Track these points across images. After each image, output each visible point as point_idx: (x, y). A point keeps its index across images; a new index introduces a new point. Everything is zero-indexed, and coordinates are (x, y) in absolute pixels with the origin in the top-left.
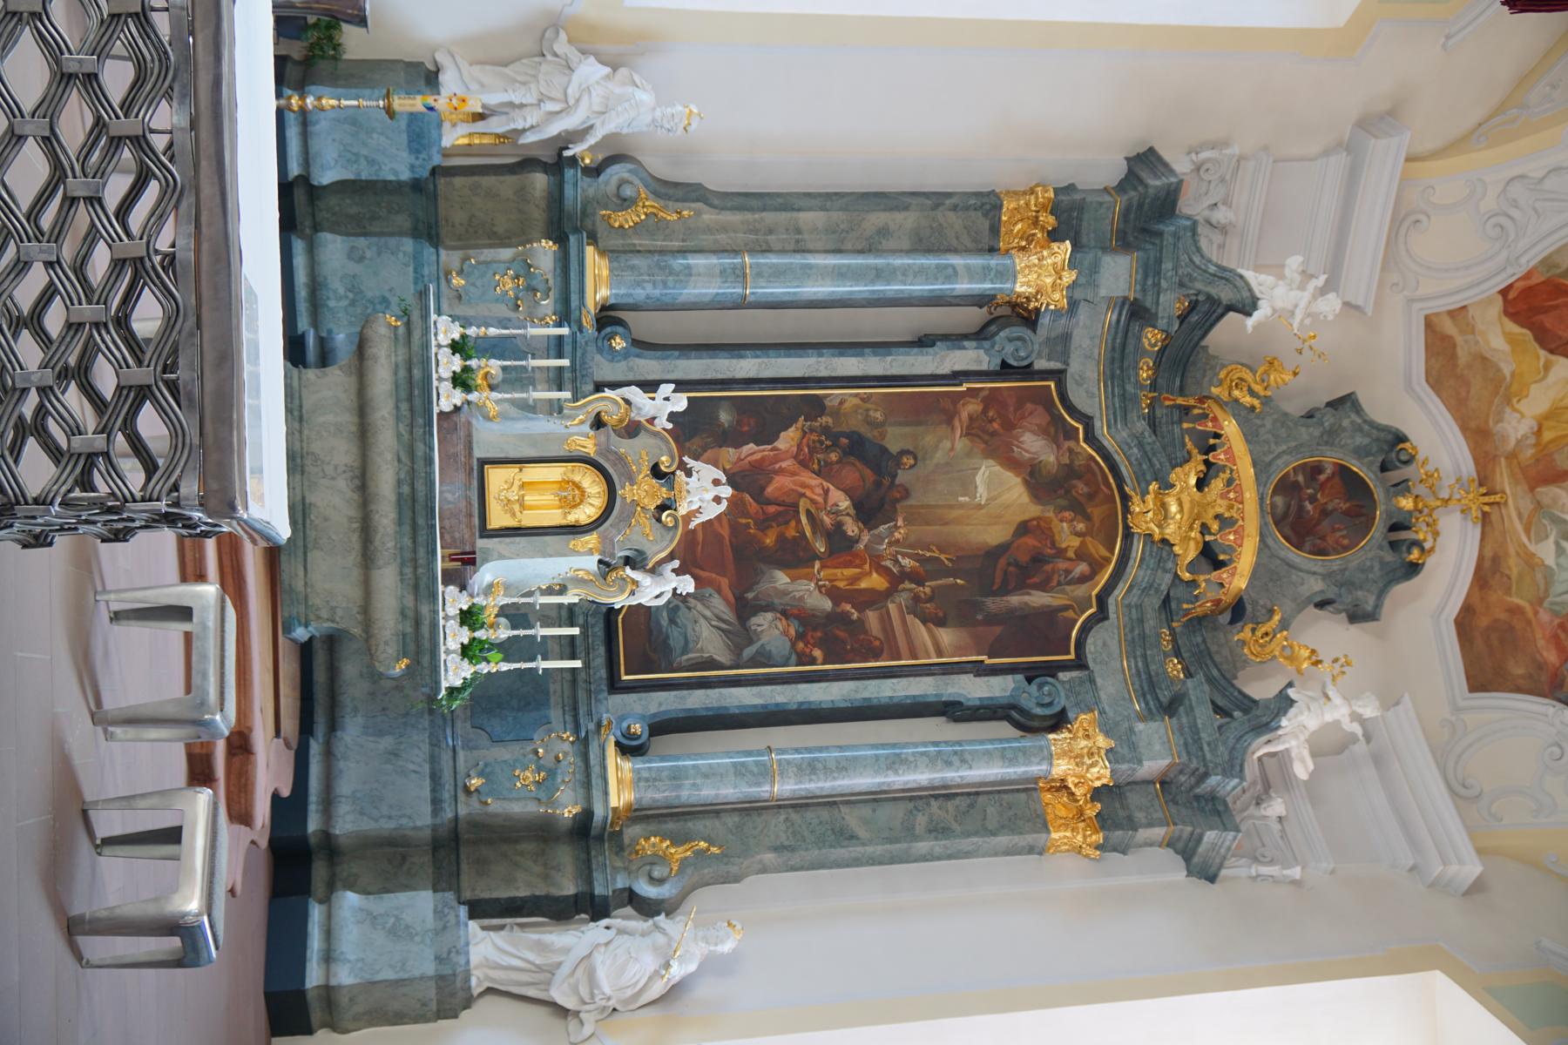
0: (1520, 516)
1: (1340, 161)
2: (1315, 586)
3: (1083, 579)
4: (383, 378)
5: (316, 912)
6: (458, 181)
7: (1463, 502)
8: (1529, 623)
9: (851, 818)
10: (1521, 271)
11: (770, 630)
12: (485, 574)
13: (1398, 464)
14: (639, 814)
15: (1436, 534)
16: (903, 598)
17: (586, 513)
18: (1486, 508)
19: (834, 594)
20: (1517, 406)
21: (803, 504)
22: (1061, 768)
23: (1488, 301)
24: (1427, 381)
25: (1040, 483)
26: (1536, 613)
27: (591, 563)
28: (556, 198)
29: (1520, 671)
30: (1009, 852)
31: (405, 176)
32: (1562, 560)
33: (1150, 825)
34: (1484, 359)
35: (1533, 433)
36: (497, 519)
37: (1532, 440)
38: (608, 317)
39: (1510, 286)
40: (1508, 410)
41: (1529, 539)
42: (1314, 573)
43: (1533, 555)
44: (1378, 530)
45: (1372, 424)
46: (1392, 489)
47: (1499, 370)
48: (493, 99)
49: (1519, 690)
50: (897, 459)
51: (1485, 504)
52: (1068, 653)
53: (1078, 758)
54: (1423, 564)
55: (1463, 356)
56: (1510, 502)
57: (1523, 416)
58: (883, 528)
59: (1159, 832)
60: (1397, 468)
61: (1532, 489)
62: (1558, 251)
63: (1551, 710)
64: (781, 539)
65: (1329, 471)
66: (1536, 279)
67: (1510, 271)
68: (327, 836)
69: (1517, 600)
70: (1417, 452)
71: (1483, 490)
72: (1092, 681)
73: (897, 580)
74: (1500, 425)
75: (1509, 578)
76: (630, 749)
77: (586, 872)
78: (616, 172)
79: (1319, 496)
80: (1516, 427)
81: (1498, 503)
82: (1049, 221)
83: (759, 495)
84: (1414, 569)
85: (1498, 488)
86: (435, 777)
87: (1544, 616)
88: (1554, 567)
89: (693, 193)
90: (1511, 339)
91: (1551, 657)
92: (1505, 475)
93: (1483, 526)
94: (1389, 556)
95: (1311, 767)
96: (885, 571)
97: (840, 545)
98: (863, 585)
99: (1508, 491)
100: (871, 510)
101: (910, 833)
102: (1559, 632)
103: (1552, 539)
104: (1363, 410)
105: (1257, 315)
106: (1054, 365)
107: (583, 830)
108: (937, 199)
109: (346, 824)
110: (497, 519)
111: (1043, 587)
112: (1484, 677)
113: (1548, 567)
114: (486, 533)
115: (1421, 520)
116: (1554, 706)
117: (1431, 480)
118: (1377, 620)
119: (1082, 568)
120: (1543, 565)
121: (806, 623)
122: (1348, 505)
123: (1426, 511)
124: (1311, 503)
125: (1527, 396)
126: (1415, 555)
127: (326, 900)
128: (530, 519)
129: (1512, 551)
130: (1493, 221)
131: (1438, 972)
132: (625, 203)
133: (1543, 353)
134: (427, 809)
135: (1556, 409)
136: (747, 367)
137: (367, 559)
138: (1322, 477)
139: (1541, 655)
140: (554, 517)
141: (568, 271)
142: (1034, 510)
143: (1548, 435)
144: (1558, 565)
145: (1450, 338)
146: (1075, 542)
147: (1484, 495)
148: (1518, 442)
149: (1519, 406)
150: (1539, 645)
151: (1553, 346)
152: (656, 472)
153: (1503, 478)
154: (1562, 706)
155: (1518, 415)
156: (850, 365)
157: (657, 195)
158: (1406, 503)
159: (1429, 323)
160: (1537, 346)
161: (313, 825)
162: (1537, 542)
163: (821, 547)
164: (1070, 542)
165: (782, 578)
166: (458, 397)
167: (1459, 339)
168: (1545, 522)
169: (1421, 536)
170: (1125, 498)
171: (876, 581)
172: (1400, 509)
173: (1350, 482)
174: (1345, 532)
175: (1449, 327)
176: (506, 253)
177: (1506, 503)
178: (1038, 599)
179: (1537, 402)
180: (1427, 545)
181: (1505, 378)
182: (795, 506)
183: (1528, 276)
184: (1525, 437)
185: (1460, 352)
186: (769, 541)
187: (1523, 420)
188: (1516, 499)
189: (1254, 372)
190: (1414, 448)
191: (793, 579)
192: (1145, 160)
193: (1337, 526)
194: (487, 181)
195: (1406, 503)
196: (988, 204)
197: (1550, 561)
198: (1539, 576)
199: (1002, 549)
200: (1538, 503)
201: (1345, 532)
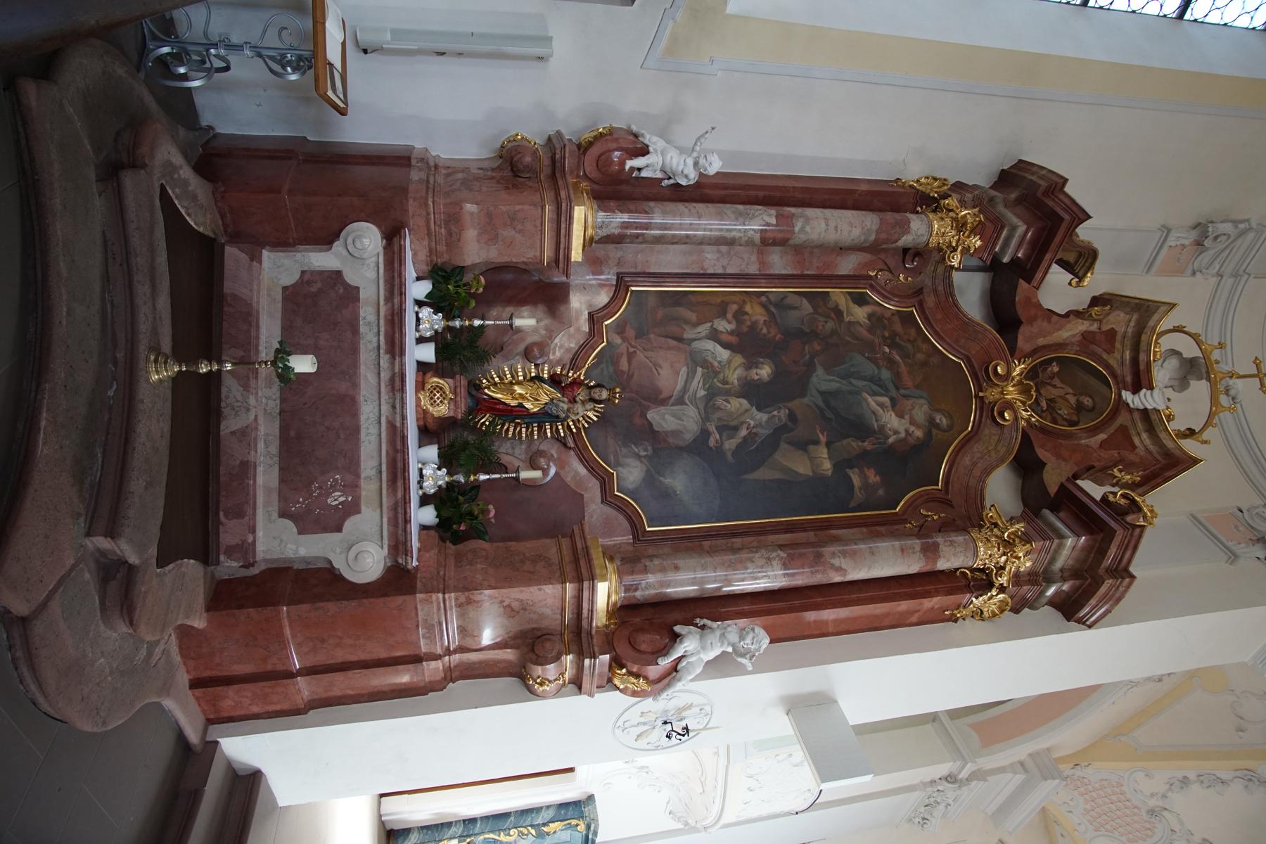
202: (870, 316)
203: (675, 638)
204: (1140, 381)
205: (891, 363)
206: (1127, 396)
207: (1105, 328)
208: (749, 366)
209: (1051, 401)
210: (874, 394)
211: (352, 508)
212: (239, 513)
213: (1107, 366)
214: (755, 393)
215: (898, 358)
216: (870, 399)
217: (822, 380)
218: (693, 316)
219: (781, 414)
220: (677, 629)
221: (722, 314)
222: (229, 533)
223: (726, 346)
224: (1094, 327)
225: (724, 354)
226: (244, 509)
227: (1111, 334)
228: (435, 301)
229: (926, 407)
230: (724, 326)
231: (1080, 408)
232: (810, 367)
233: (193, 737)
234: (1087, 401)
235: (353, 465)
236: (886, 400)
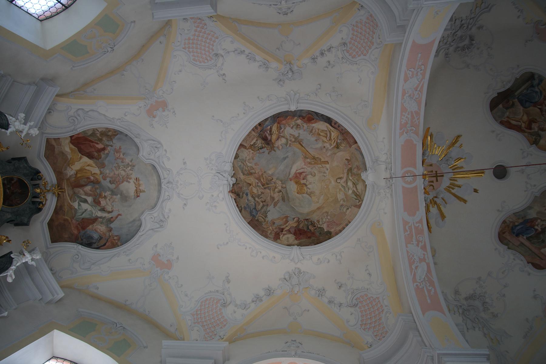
0: (69, 195)
1: (33, 88)
2: (9, 216)
7: (54, 191)
8: (70, 223)
10: (77, 133)
13: (37, 179)
15: (46, 200)
18: (60, 193)
20: (71, 167)
23: (66, 138)
24: (45, 156)
26: (72, 221)
29: (66, 236)
32: (80, 207)
34: (63, 153)
35: (75, 174)
37: (74, 176)
39: (73, 136)
40: (68, 168)
41: (71, 201)
42: (8, 212)
43: (72, 206)
44: (29, 199)
45: (30, 167)
46: (34, 186)
47: (67, 157)
49: (66, 241)
51: (59, 192)
54: (42, 209)
56: (66, 192)
57: (72, 169)
60: (37, 180)
61: (73, 189)
62: (88, 130)
63: (75, 246)
65: (15, 180)
66: (80, 136)
67: (74, 132)
69: (66, 217)
70: (43, 177)
71: (59, 188)
74: (65, 171)
75: (64, 211)
79: (11, 188)
80: (70, 172)
81: (63, 192)
84: (40, 210)
85: (63, 187)
87: (74, 221)
88: (77, 209)
90: (71, 149)
91: (76, 232)
92: (66, 184)
93: (58, 197)
95: (14, 277)
99: (66, 188)
102: (78, 226)
103: (77, 201)
104: (28, 163)
105: (10, 130)
112: (55, 239)
113: (76, 209)
115: (42, 195)
116: (76, 245)
117: (45, 184)
118: (29, 225)
120: (75, 208)
122: (20, 191)
123: (43, 193)
124: (8, 190)
125: (74, 164)
129: (66, 204)
130: (72, 118)
131: (55, 330)
133: (80, 155)
135: (82, 169)
138: (13, 182)
139: (73, 231)
143: (79, 175)
144: (78, 208)
145: (54, 146)
147: (59, 189)
148: (70, 176)
149: (72, 167)
150: (72, 229)
151: (83, 153)
153: (65, 185)
154: (78, 245)
155: (71, 169)
158: (38, 191)
159: (48, 140)
160: (78, 152)
162: (73, 203)
167: (56, 146)
168: (76, 197)
169: (42, 201)
172: (36, 192)
173: (21, 183)
174: (19, 199)
175: (53, 143)
177: (65, 192)
179: (77, 166)
180: (44, 203)
181: (68, 159)
183: (78, 134)
184: (72, 175)
185: (56, 150)
187: (72, 171)
188: (68, 191)
190: (42, 175)
193: (17, 197)
195: (38, 191)
197: (76, 207)
198: (73, 211)
200: (74, 192)
201: (19, 199)
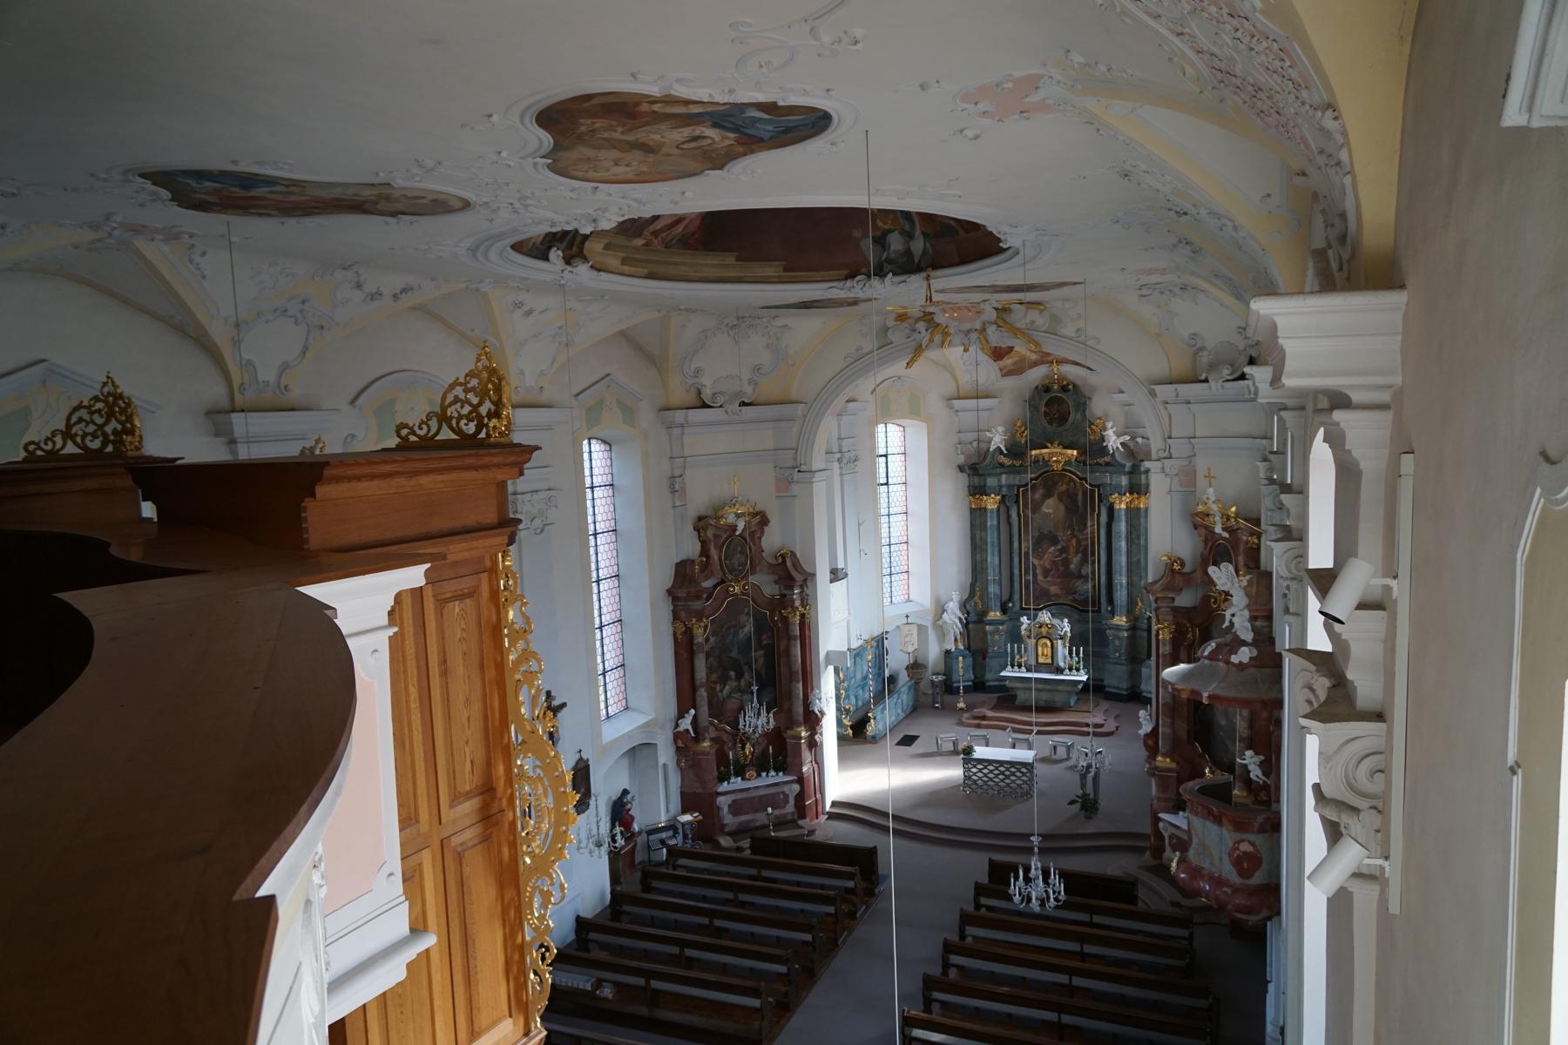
2: (1079, 416)
3: (1075, 484)
4: (1018, 685)
5: (1145, 694)
6: (972, 644)
9: (1134, 559)
11: (1087, 570)
12: (1062, 664)
14: (1130, 611)
16: (1079, 534)
17: (1049, 643)
19: (1077, 553)
21: (1053, 559)
22: (1123, 506)
25: (1048, 495)
27: (1059, 641)
28: (974, 622)
30: (1146, 517)
31: (971, 659)
33: (1140, 479)
36: (1049, 661)
38: (1004, 610)
48: (953, 639)
50: (1041, 533)
52: (1095, 491)
53: (1120, 503)
55: (1012, 368)
58: (1060, 538)
59: (1143, 477)
64: (1062, 566)
68: (1127, 690)
72: (1102, 485)
73: (1073, 536)
76: (1113, 613)
77: (1142, 630)
78: (968, 607)
82: (977, 496)
83: (1051, 570)
84: (1075, 386)
86: (1116, 663)
89: (973, 586)
94: (1070, 393)
96: (1071, 538)
97: (1063, 550)
98: (1074, 544)
100: (1054, 540)
101: (1139, 545)
106: (1016, 488)
107: (1133, 628)
108: (972, 526)
109: (1125, 685)
110: (1049, 661)
111: (1077, 495)
114: (1053, 664)
119: (1072, 484)
121: (1084, 561)
126: (1071, 387)
127: (1142, 692)
128: (1050, 655)
132: (976, 604)
134: (1123, 667)
136: (1016, 572)
137: (1058, 691)
140: (1049, 650)
141: (991, 623)
142: (1056, 496)
146: (1064, 486)
152: (1040, 627)
156: (1016, 545)
157: (974, 596)
159: (1003, 376)
161: (1125, 693)
163: (1064, 555)
164: (1064, 487)
165: (1072, 566)
166: (1023, 668)
170: (1053, 470)
171: (1074, 542)
176: (989, 637)
178: (1080, 497)
182: (1054, 562)
186: (1062, 569)
189: (1017, 431)
191: (1072, 563)
192: (961, 468)
194: (971, 638)
196: (972, 511)
199: (1066, 507)
202: (713, 636)
203: (813, 711)
204: (734, 528)
205: (729, 628)
206: (737, 533)
207: (713, 539)
208: (731, 679)
209: (740, 565)
210: (739, 635)
211: (784, 793)
212: (785, 816)
213: (727, 539)
214: (739, 676)
215: (726, 626)
216: (741, 636)
217: (734, 654)
218: (716, 698)
219: (746, 668)
220: (811, 709)
221: (715, 688)
222: (790, 817)
223: (724, 687)
224: (713, 543)
225: (727, 687)
226: (785, 815)
227: (716, 536)
228: (728, 779)
229: (743, 616)
230: (718, 687)
231: (741, 552)
232: (731, 657)
233: (826, 817)
234: (739, 549)
235: (774, 794)
236: (741, 631)
